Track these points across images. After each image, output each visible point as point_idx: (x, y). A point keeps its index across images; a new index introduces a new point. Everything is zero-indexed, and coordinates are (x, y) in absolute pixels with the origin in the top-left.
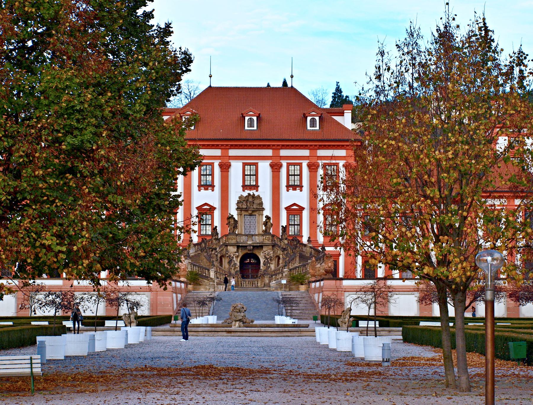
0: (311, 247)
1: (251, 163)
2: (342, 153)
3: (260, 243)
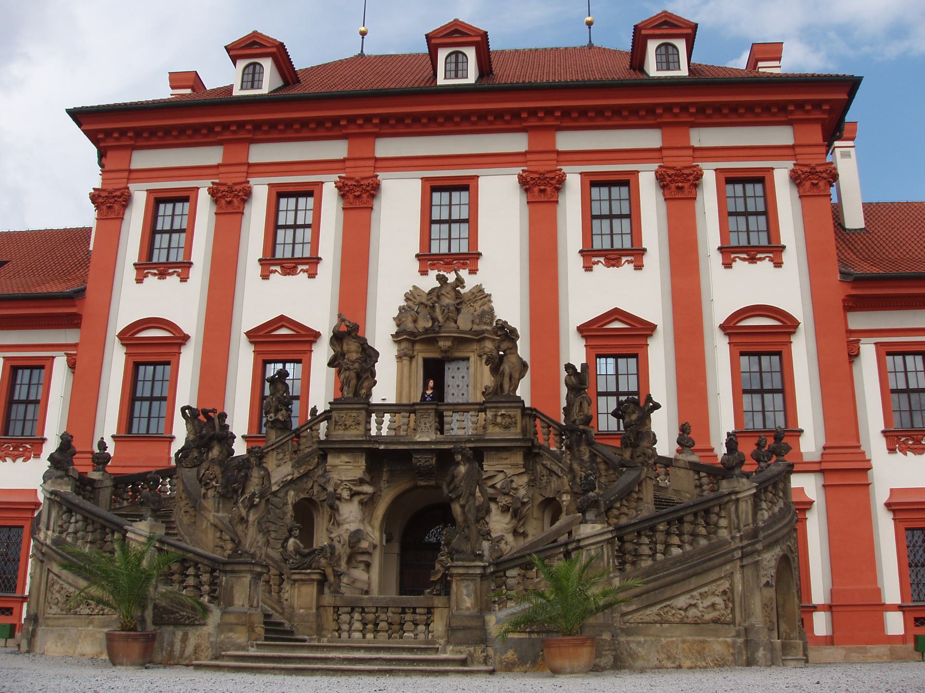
0: (695, 467)
1: (450, 185)
2: (782, 136)
3: (469, 441)
